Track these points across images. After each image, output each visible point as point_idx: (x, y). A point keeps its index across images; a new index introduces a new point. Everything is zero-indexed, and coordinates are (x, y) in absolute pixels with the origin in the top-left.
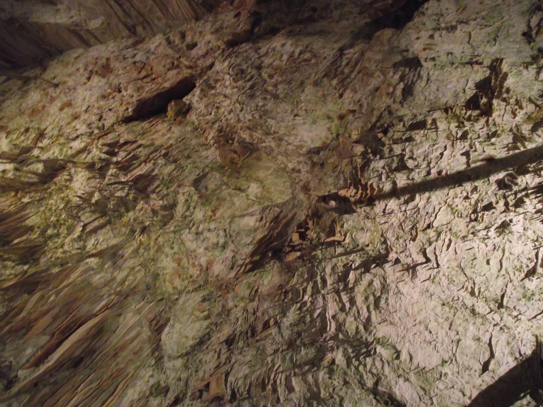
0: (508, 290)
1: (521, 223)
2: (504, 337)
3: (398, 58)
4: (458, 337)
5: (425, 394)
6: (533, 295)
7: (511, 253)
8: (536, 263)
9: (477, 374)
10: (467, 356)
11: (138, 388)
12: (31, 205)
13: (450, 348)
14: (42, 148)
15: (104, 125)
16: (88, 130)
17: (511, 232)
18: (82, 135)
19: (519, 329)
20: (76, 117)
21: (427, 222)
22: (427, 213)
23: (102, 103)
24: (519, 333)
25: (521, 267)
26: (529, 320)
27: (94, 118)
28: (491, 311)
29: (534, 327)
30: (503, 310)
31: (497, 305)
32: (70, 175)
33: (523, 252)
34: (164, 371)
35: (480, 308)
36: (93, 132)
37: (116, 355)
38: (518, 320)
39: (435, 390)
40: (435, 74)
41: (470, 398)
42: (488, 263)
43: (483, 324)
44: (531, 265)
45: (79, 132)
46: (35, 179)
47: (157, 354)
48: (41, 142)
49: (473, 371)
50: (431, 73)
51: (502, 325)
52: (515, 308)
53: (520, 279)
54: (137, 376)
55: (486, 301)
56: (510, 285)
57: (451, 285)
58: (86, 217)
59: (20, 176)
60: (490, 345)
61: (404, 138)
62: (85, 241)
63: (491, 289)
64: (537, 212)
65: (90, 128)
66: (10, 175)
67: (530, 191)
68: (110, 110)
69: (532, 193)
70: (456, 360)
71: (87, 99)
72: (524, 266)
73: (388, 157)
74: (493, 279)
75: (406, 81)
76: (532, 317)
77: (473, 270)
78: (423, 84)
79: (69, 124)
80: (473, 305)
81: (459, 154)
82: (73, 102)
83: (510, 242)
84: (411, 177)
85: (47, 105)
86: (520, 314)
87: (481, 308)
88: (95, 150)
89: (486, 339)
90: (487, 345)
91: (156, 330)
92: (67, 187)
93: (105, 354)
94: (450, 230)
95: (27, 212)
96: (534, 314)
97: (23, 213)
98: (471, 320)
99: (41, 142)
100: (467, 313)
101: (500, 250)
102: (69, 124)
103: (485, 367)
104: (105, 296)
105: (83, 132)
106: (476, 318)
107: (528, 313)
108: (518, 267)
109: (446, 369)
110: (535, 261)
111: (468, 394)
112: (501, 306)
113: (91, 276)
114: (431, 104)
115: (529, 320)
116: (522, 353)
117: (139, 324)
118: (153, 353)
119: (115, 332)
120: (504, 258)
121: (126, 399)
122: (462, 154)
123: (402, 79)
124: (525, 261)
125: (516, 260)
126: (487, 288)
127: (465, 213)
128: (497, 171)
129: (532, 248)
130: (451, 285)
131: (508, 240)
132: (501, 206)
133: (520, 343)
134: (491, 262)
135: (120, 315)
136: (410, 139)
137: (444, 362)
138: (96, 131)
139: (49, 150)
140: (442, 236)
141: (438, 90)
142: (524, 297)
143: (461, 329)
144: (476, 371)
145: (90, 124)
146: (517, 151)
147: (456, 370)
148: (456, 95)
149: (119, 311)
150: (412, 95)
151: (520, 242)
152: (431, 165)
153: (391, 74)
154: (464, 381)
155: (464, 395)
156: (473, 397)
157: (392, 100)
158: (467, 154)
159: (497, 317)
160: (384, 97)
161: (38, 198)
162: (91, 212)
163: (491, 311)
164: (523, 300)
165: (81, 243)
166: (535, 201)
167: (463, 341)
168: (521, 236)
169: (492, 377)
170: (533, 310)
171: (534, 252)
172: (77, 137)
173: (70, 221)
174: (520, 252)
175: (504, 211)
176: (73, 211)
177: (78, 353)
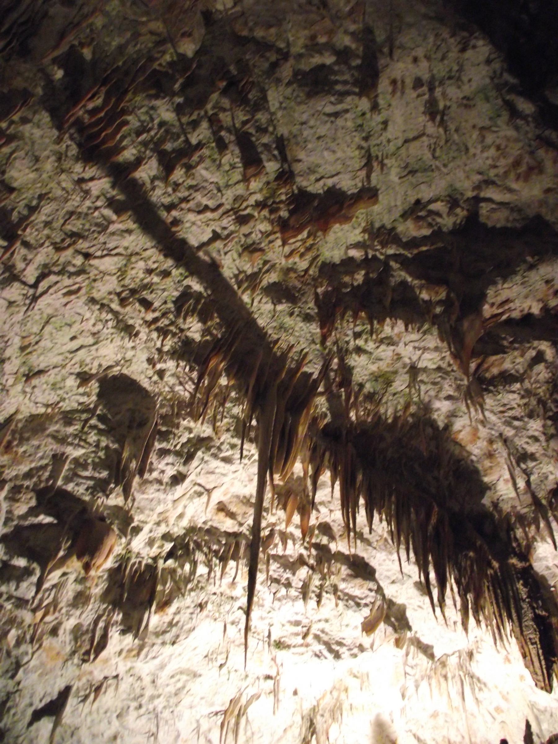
3: (380, 36)
6: (60, 388)
21: (91, 250)
22: (105, 243)
25: (87, 365)
40: (348, 122)
50: (348, 116)
53: (72, 371)
57: (19, 325)
61: (223, 133)
63: (42, 358)
72: (90, 366)
73: (182, 125)
75: (336, 68)
77: (54, 331)
78: (329, 109)
81: (213, 228)
84: (157, 183)
94: (95, 280)
114: (295, 136)
122: (214, 232)
123: (343, 55)
124: (96, 364)
127: (127, 282)
128: (201, 279)
130: (19, 325)
132: (150, 316)
136: (222, 146)
140: (79, 279)
141: (319, 138)
142: (54, 384)
146: (236, 287)
148: (311, 170)
150: (310, 95)
152: (183, 205)
153: (353, 28)
157: (303, 51)
158: (216, 236)
160: (306, 32)
175: (146, 322)
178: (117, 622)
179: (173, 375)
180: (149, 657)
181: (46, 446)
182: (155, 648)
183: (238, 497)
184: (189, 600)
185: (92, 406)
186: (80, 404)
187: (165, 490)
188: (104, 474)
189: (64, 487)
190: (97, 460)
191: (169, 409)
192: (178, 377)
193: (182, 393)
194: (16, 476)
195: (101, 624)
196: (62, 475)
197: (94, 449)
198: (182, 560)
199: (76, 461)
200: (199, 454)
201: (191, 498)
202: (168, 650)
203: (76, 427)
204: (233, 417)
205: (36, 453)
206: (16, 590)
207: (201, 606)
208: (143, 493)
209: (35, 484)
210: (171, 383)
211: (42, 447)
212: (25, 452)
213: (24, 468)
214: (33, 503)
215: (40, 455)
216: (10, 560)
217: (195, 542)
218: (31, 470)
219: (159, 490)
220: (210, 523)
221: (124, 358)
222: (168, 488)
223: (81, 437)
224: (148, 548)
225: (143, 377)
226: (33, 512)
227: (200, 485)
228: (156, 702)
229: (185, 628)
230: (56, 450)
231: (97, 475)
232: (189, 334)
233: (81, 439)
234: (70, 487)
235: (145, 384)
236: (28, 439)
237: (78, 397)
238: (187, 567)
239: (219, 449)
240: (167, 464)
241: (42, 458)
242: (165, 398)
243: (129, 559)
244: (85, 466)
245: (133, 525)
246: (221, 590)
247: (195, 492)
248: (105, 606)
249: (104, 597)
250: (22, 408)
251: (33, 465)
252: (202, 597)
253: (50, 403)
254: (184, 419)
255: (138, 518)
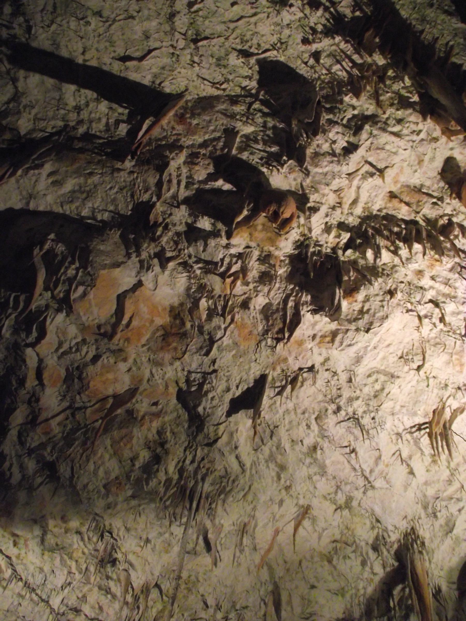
0: (215, 41)
1: (293, 18)
2: (166, 61)
4: (135, 14)
5: (52, 13)
6: (225, 67)
7: (256, 24)
8: (258, 54)
9: (113, 55)
10: (123, 34)
13: (118, 12)
17: (278, 12)
19: (183, 71)
24: (180, 73)
25: (247, 41)
26: (198, 76)
28: (184, 35)
29: (195, 83)
30: (193, 46)
31: (194, 37)
33: (263, 36)
35: (180, 22)
38: (192, 65)
39: (64, 22)
41: (85, 61)
42: (233, 4)
43: (165, 33)
44: (253, 50)
49: (112, 49)
51: (178, 53)
52: (201, 56)
55: (191, 24)
56: (222, 39)
60: (150, 52)
64: (311, 28)
67: (332, 10)
69: (331, 13)
70: (110, 25)
74: (220, 19)
76: (203, 76)
80: (179, 12)
83: (268, 17)
86: (198, 64)
87: (181, 22)
89: (153, 44)
90: (147, 48)
96: (207, 77)
98: (162, 19)
100: (167, 10)
101: (254, 11)
103: (125, 59)
106: (167, 22)
107: (204, 71)
108: (245, 38)
109: (94, 21)
110: (260, 52)
111: (88, 56)
112: (195, 41)
115: (198, 76)
116: (162, 85)
120: (247, 20)
124: (255, 41)
125: (251, 33)
126: (206, 18)
129: (272, 43)
131: (269, 14)
133: (171, 78)
134: (235, 7)
137: (99, 14)
142: (219, 59)
143: (146, 12)
144: (115, 52)
147: (101, 30)
151: (273, 27)
154: (96, 46)
155: (83, 53)
156: (88, 63)
159: (182, 44)
163: (184, 35)
164: (214, 60)
166: (323, 21)
167: (135, 22)
168: (279, 25)
169: (121, 71)
170: (210, 74)
171: (268, 47)
174: (261, 33)
178: (307, 302)
179: (328, 56)
180: (345, 344)
181: (216, 120)
182: (350, 334)
183: (408, 186)
184: (378, 285)
185: (254, 91)
186: (243, 88)
187: (339, 161)
188: (274, 149)
189: (239, 156)
190: (266, 138)
191: (329, 90)
192: (334, 56)
193: (340, 73)
194: (193, 146)
195: (291, 304)
196: (236, 145)
197: (262, 129)
198: (361, 249)
199: (247, 137)
200: (367, 127)
201: (364, 178)
202: (363, 339)
203: (243, 108)
204: (393, 92)
205: (208, 127)
206: (204, 251)
207: (391, 293)
208: (316, 166)
209: (211, 152)
210: (327, 65)
211: (213, 121)
212: (198, 124)
213: (199, 139)
214: (211, 169)
215: (212, 128)
216: (195, 222)
217: (373, 228)
218: (205, 141)
219: (332, 162)
220: (385, 211)
221: (280, 40)
222: (342, 158)
223: (248, 116)
224: (326, 235)
225: (299, 62)
226: (211, 177)
227: (371, 164)
228: (356, 404)
229: (377, 315)
230: (226, 126)
231: (268, 149)
232: (340, 9)
233: (248, 118)
234: (245, 156)
235: (303, 70)
236: (199, 115)
237: (241, 79)
238: (370, 254)
239: (385, 123)
240: (338, 133)
241: (214, 131)
242: (323, 82)
243: (308, 246)
244: (256, 141)
245: (309, 205)
246: (409, 278)
247: (367, 172)
248: (292, 286)
249: (290, 278)
250: (191, 89)
251: (207, 137)
252: (390, 284)
253: (216, 81)
254: (346, 95)
255: (314, 198)
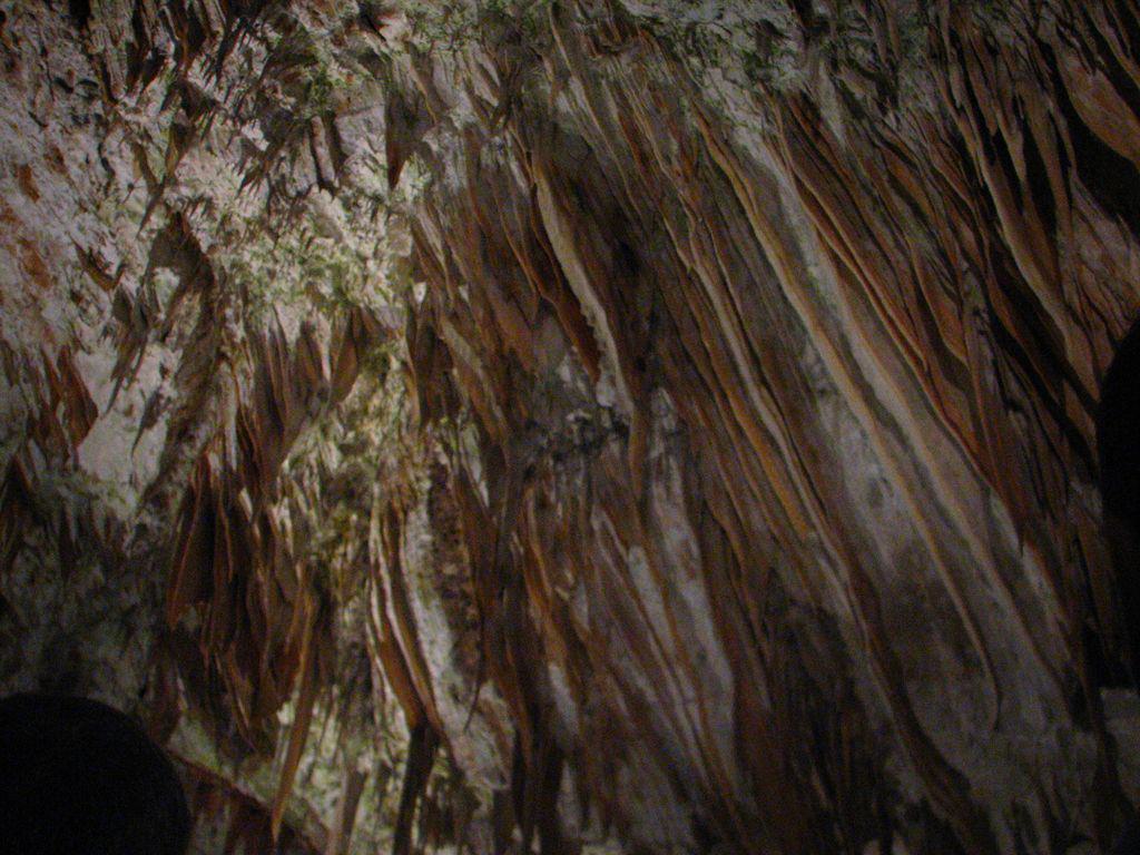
11: (740, 115)
12: (253, 321)
14: (123, 267)
15: (85, 82)
16: (92, 127)
18: (100, 148)
20: (56, 160)
23: (25, 75)
27: (61, 105)
32: (194, 203)
34: (724, 35)
36: (98, 117)
37: (645, 159)
45: (94, 156)
46: (192, 304)
47: (679, 48)
48: (108, 266)
54: (712, 112)
58: (303, 176)
59: (181, 336)
62: (361, 191)
65: (87, 121)
66: (174, 360)
68: (45, 53)
71: (13, 118)
79: (72, 183)
82: (20, 162)
85: (20, 233)
88: (143, 120)
91: (624, 36)
92: (226, 219)
93: (633, 186)
95: (268, 335)
97: (267, 344)
99: (108, 266)
102: (72, 183)
104: (501, 161)
105: (95, 143)
113: (445, 188)
117: (592, 82)
118: (675, 58)
119: (590, 149)
121: (754, 152)
135: (556, 127)
138: (98, 107)
139: (130, 250)
145: (75, 118)
149: (547, 127)
161: (240, 302)
162: (293, 161)
165: (365, 204)
172: (105, 162)
173: (305, 224)
176: (286, 205)
177: (607, 256)
